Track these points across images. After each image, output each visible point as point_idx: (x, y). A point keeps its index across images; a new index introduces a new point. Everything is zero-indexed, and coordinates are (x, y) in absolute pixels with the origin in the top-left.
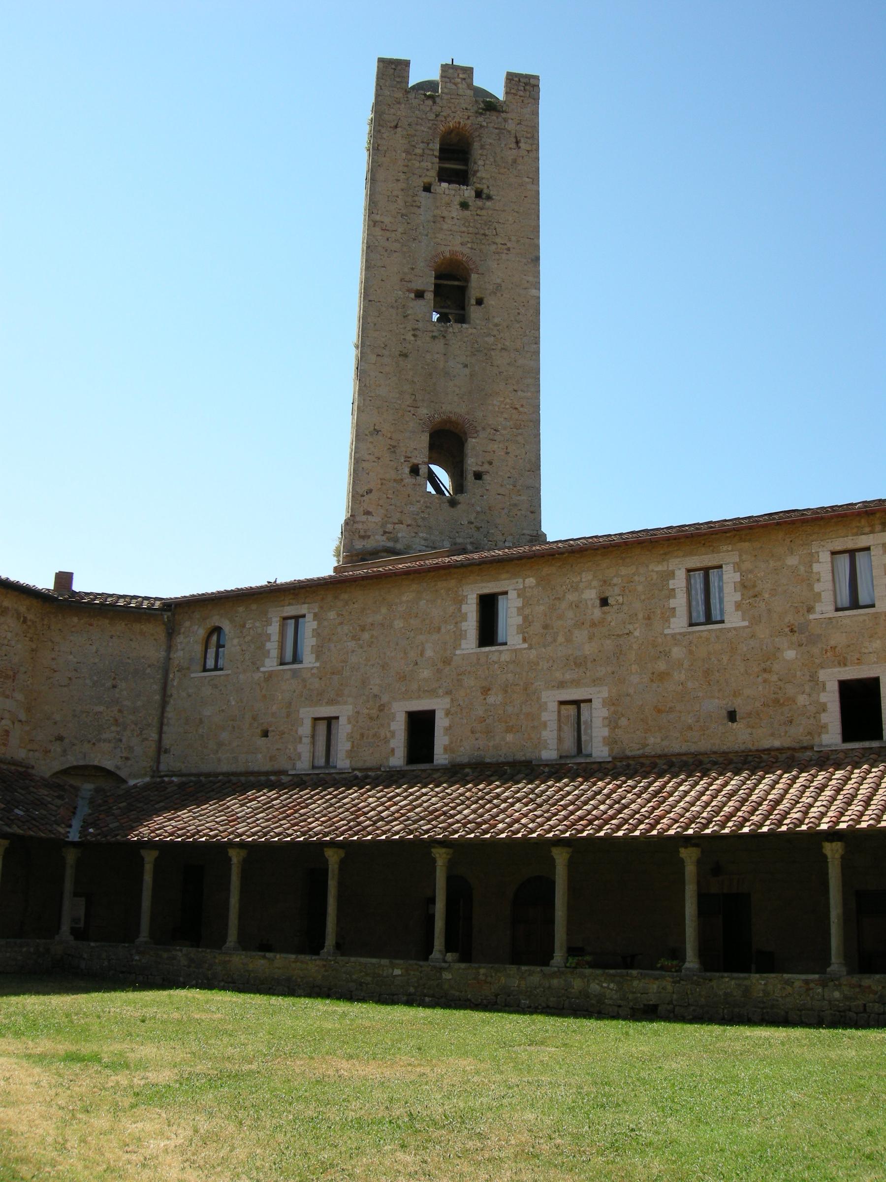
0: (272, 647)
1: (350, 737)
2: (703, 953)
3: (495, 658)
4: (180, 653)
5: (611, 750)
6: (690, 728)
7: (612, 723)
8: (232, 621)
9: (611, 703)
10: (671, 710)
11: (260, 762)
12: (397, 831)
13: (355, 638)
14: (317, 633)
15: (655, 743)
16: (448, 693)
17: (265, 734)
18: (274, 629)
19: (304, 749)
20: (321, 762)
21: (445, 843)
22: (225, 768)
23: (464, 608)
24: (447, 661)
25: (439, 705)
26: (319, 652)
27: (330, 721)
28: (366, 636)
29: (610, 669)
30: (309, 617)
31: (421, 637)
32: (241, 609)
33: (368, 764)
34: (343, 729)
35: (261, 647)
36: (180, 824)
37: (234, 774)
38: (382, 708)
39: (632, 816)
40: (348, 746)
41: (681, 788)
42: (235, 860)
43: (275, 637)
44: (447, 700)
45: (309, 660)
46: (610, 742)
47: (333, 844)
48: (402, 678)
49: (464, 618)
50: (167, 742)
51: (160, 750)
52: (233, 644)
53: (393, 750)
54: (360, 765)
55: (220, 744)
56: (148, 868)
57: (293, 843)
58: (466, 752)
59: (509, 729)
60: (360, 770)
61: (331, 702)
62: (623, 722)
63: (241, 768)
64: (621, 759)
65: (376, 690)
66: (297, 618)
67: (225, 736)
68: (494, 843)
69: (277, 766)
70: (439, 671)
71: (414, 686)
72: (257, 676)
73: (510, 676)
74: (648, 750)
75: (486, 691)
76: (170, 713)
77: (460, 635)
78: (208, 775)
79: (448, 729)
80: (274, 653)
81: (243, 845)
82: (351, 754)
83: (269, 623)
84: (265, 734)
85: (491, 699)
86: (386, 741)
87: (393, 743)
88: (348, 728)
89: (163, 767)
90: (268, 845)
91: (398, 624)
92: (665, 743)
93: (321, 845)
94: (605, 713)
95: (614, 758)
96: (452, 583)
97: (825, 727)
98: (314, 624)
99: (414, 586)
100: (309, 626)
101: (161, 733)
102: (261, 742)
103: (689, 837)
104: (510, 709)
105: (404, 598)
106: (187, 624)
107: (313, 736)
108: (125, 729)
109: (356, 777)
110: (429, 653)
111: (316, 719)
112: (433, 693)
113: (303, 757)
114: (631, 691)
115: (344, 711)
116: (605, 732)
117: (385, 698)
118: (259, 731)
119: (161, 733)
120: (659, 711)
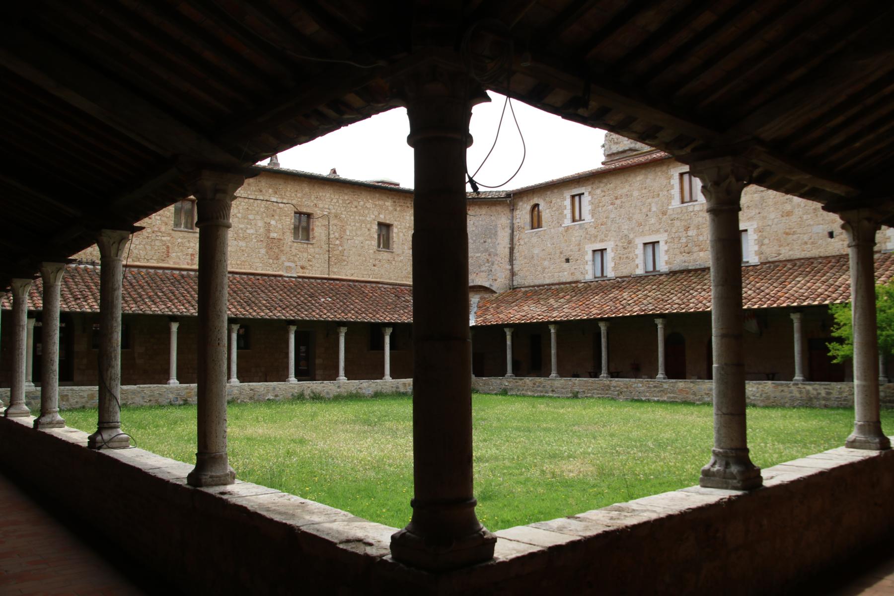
0: (568, 212)
1: (613, 259)
2: (803, 372)
3: (691, 209)
4: (518, 220)
5: (760, 258)
6: (806, 243)
7: (761, 243)
8: (544, 200)
9: (759, 230)
10: (794, 233)
11: (566, 277)
12: (636, 310)
13: (612, 204)
14: (591, 203)
15: (786, 253)
16: (666, 231)
17: (567, 260)
18: (568, 202)
19: (589, 267)
20: (599, 274)
21: (661, 316)
22: (547, 281)
23: (672, 182)
24: (664, 213)
25: (661, 237)
26: (593, 213)
27: (602, 251)
28: (618, 202)
29: (757, 211)
30: (586, 194)
31: (649, 200)
32: (549, 193)
33: (624, 274)
34: (609, 256)
35: (562, 213)
36: (523, 314)
37: (553, 284)
38: (630, 242)
39: (764, 297)
40: (613, 264)
41: (798, 279)
42: (553, 331)
43: (569, 207)
44: (666, 234)
45: (587, 217)
46: (760, 253)
47: (602, 319)
48: (640, 225)
49: (672, 187)
50: (516, 269)
51: (513, 274)
52: (546, 213)
53: (637, 266)
54: (620, 275)
55: (544, 269)
56: (509, 338)
57: (581, 320)
58: (678, 263)
59: (701, 250)
60: (620, 277)
61: (602, 241)
62: (766, 241)
63: (556, 281)
64: (765, 263)
65: (626, 232)
66: (580, 195)
67: (546, 263)
68: (687, 314)
69: (575, 279)
70: (660, 219)
71: (647, 228)
72: (561, 229)
73: (700, 219)
74: (781, 257)
75: (687, 229)
76: (516, 254)
77: (670, 198)
78: (538, 286)
79: (667, 251)
80: (569, 216)
81: (555, 323)
82: (615, 268)
83: (564, 199)
84: (567, 260)
85: (690, 233)
86: (633, 260)
87: (637, 261)
88: (612, 255)
89: (515, 283)
90: (569, 322)
91: (636, 194)
92: (791, 253)
93: (596, 320)
94: (756, 237)
95: (762, 263)
96: (664, 168)
97: (889, 238)
98: (589, 198)
99: (643, 171)
100: (586, 199)
101: (512, 264)
102: (566, 265)
103: (794, 307)
104: (701, 238)
105: (638, 179)
106: (521, 204)
107: (594, 260)
108: (493, 264)
109: (618, 282)
110: (654, 209)
111: (594, 251)
112: (657, 231)
113: (588, 273)
114: (770, 223)
115: (609, 245)
116: (756, 248)
117: (631, 236)
118: (564, 260)
119: (512, 264)
120: (787, 234)
